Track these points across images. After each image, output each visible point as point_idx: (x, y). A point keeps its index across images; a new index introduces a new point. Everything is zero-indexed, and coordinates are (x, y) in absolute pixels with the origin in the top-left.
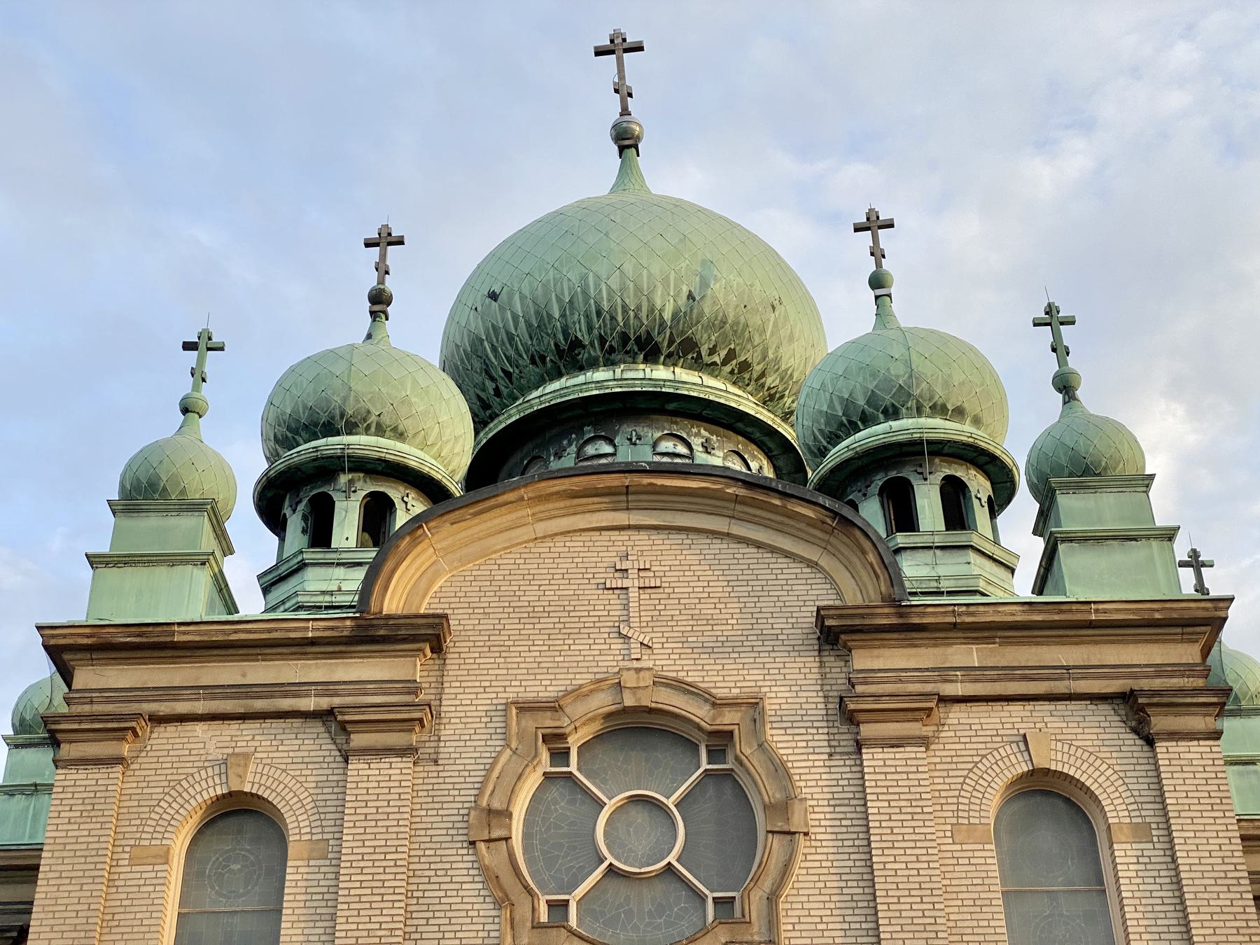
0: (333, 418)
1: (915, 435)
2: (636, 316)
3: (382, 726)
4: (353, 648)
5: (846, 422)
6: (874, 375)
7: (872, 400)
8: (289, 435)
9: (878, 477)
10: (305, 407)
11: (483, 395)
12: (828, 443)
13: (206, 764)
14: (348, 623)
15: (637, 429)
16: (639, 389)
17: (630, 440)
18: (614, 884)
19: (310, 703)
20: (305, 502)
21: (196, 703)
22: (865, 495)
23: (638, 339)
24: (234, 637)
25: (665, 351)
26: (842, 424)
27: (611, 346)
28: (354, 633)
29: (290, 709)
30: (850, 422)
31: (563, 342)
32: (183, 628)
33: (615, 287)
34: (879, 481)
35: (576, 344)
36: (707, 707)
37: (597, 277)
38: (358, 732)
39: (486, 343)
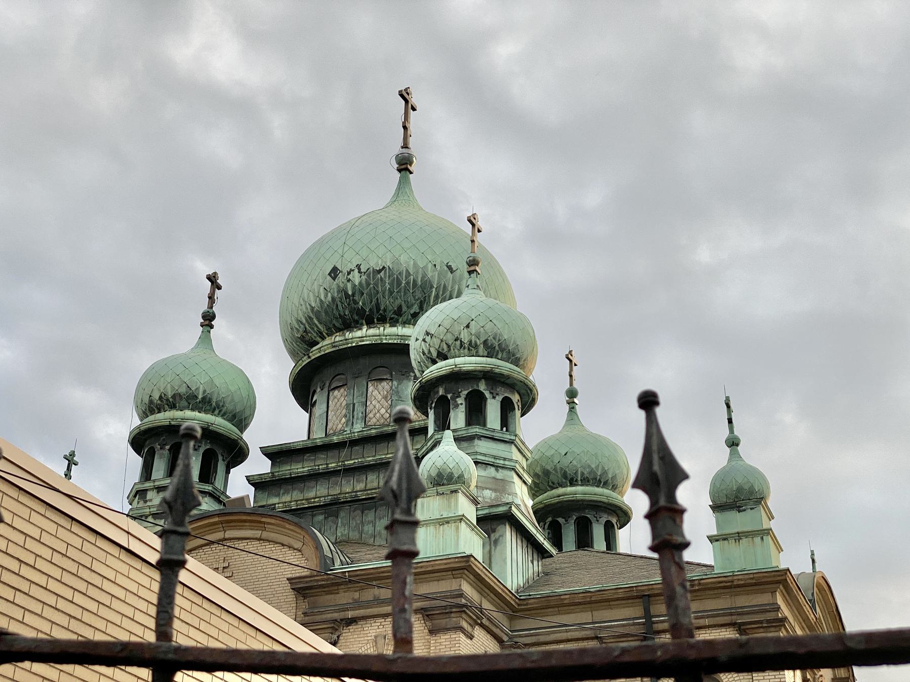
0: (522, 358)
5: (598, 479)
8: (497, 348)
9: (605, 516)
10: (515, 342)
11: (404, 309)
12: (581, 480)
22: (598, 521)
24: (804, 607)
26: (596, 479)
34: (604, 519)
39: (434, 290)
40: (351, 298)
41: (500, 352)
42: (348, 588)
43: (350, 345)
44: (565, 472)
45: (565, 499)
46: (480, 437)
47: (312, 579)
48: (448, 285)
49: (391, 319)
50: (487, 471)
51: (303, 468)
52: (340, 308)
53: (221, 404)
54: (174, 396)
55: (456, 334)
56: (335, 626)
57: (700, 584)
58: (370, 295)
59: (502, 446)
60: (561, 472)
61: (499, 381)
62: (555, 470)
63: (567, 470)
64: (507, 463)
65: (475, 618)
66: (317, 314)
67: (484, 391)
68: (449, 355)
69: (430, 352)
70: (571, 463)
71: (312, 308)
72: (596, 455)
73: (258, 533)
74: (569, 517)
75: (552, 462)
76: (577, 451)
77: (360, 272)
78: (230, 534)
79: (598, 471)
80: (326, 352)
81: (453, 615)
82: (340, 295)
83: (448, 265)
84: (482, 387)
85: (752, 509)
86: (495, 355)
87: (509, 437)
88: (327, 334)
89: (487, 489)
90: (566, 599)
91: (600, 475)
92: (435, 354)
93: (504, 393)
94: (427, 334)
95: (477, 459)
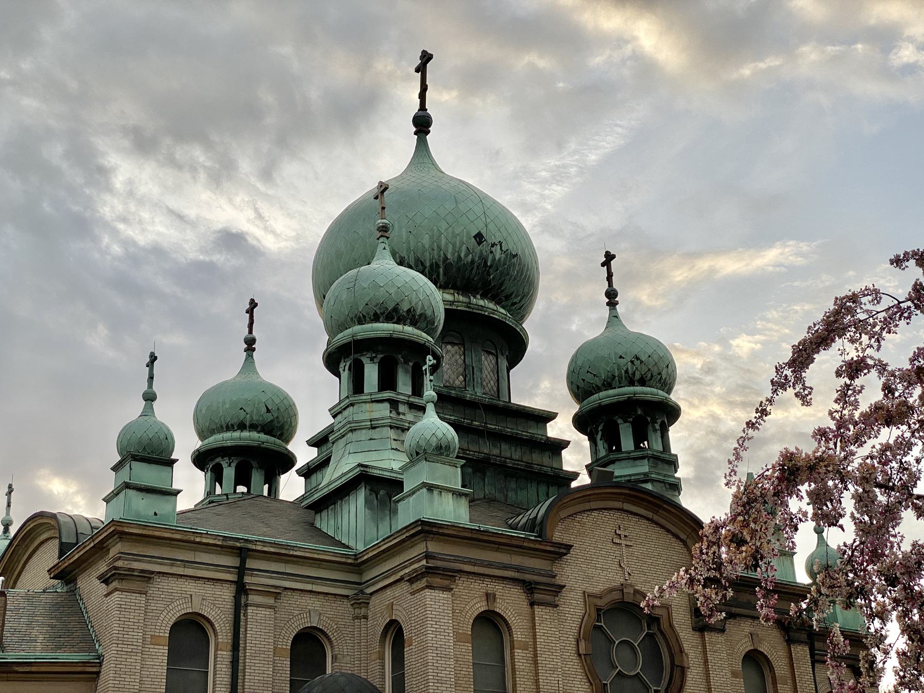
11: (513, 296)
40: (487, 269)
43: (483, 313)
49: (500, 299)
51: (451, 416)
52: (474, 272)
54: (421, 315)
58: (502, 273)
66: (448, 266)
68: (647, 383)
69: (634, 374)
71: (446, 258)
73: (650, 515)
78: (627, 506)
80: (459, 308)
82: (479, 261)
88: (440, 285)
92: (638, 376)
94: (637, 358)
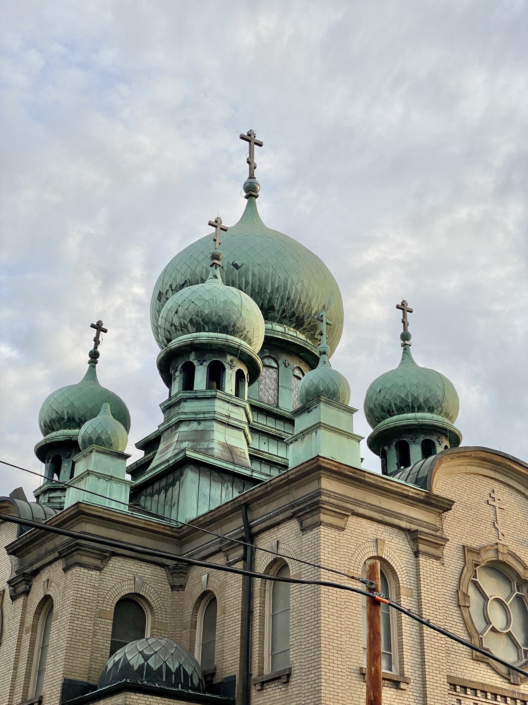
0: (229, 325)
1: (444, 426)
2: (302, 307)
3: (429, 544)
4: (421, 505)
5: (410, 406)
6: (430, 391)
7: (426, 401)
9: (422, 436)
10: (217, 314)
12: (396, 410)
13: (369, 540)
14: (424, 494)
15: (289, 360)
16: (298, 343)
17: (285, 364)
18: (493, 634)
19: (404, 524)
20: (208, 362)
21: (366, 510)
23: (298, 317)
24: (386, 486)
25: (304, 327)
27: (286, 315)
28: (425, 499)
29: (397, 524)
30: (412, 406)
31: (266, 305)
32: (369, 475)
33: (299, 290)
34: (422, 438)
35: (272, 308)
36: (522, 568)
37: (292, 281)
38: (421, 543)
41: (205, 326)
42: (35, 546)
44: (382, 407)
45: (381, 430)
46: (185, 400)
47: (15, 544)
48: (236, 279)
50: (191, 426)
53: (83, 419)
55: (170, 320)
56: (26, 578)
57: (271, 485)
59: (205, 403)
60: (379, 407)
61: (207, 350)
62: (375, 406)
63: (383, 404)
64: (206, 415)
65: (98, 552)
67: (193, 361)
70: (384, 397)
72: (404, 386)
74: (391, 444)
75: (372, 400)
76: (388, 386)
77: (172, 290)
79: (408, 399)
81: (75, 553)
83: (235, 263)
84: (192, 358)
85: (315, 408)
86: (202, 329)
87: (210, 393)
89: (185, 441)
90: (201, 520)
91: (411, 402)
92: (166, 342)
93: (211, 358)
95: (179, 418)
